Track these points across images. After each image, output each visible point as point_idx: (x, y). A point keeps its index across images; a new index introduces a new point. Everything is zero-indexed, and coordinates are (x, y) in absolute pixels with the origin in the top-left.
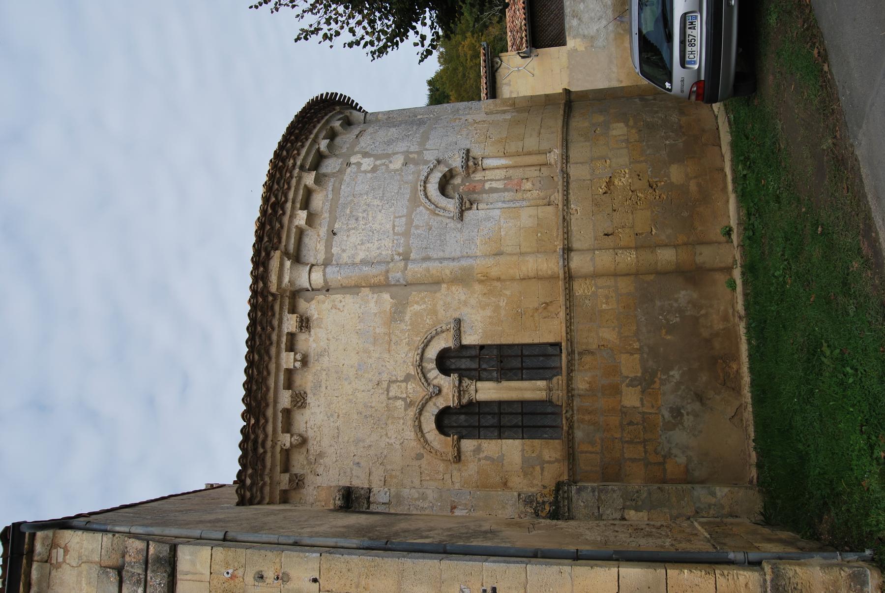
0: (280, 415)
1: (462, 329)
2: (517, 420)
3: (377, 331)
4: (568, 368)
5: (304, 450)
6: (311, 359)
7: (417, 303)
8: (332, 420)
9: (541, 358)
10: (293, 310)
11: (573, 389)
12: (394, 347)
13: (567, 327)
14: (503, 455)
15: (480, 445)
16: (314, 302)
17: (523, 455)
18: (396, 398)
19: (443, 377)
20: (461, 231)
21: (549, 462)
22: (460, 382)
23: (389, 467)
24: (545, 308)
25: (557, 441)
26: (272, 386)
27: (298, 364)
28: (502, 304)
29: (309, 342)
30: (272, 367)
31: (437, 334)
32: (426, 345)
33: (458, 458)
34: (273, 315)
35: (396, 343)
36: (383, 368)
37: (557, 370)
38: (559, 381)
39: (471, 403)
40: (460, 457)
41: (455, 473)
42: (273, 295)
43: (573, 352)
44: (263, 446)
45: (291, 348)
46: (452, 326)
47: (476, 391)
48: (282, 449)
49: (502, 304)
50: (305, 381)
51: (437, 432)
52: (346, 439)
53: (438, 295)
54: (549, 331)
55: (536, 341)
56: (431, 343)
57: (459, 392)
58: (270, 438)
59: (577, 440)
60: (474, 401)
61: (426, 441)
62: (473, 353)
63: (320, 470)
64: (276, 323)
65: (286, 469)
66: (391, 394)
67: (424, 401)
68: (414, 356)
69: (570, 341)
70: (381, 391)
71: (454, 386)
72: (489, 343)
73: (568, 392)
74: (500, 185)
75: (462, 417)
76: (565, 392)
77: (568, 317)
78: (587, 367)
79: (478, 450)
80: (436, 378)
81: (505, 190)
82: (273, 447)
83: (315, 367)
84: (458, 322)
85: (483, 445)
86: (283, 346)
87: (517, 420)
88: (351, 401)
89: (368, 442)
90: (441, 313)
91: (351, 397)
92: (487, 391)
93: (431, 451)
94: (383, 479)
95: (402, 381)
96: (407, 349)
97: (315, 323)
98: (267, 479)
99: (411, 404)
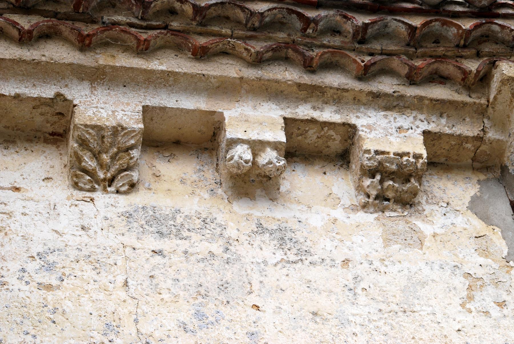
0: (48, 92)
6: (261, 211)
8: (32, 266)
26: (160, 64)
29: (321, 203)
30: (229, 69)
42: (484, 79)
50: (176, 186)
64: (386, 85)
83: (237, 217)
86: (304, 111)
97: (401, 226)
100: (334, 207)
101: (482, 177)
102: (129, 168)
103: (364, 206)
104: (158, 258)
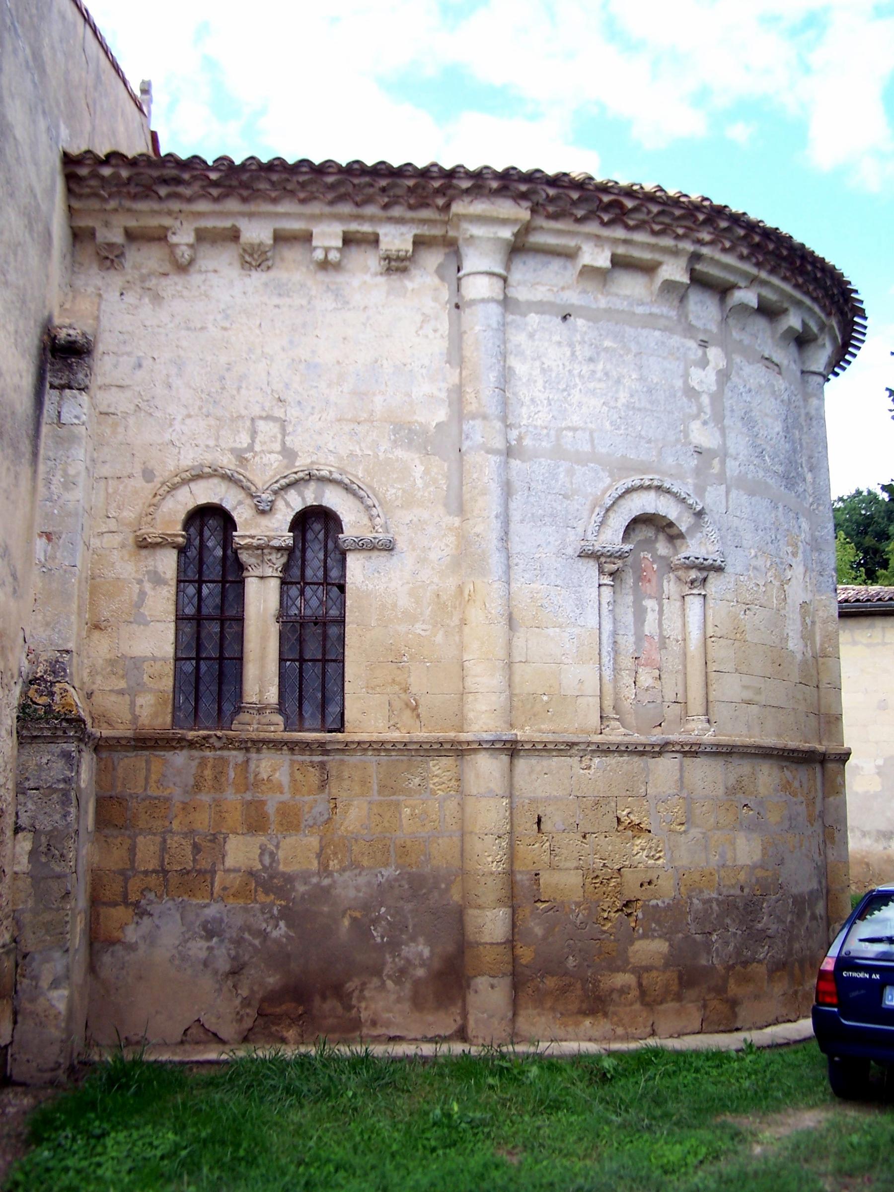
0: (227, 224)
1: (375, 553)
2: (211, 650)
3: (378, 400)
4: (297, 743)
5: (167, 267)
7: (427, 472)
8: (219, 317)
9: (319, 695)
10: (419, 242)
11: (259, 751)
12: (347, 428)
13: (371, 743)
14: (146, 624)
15: (165, 583)
16: (436, 280)
17: (144, 659)
18: (254, 433)
19: (290, 518)
20: (560, 553)
21: (133, 704)
22: (279, 549)
23: (131, 421)
24: (407, 705)
25: (169, 719)
27: (319, 255)
28: (419, 628)
31: (368, 508)
32: (347, 488)
33: (144, 545)
34: (411, 207)
35: (353, 433)
36: (309, 410)
37: (295, 721)
39: (241, 567)
40: (145, 547)
41: (117, 539)
42: (447, 207)
43: (326, 752)
44: (170, 196)
45: (348, 240)
46: (381, 536)
47: (262, 578)
48: (166, 229)
49: (419, 628)
51: (191, 506)
52: (184, 344)
53: (441, 510)
54: (366, 711)
55: (347, 686)
56: (351, 497)
57: (258, 547)
58: (185, 207)
59: (169, 755)
60: (245, 574)
61: (174, 487)
62: (334, 574)
63: (130, 298)
64: (397, 211)
65: (131, 236)
66: (261, 425)
67: (245, 483)
69: (347, 748)
70: (267, 405)
71: (270, 539)
72: (348, 603)
73: (254, 742)
74: (650, 626)
75: (219, 552)
76: (254, 736)
77: (389, 747)
78: (298, 776)
79: (157, 580)
80: (288, 505)
81: (640, 637)
82: (170, 213)
83: (316, 283)
84: (389, 547)
87: (211, 650)
88: (251, 350)
89: (177, 382)
90: (405, 516)
91: (259, 351)
93: (158, 498)
94: (112, 410)
95: (283, 443)
96: (344, 453)
98: (112, 204)
99: (242, 460)
100: (366, 273)
101: (447, 250)
102: (267, 260)
103: (381, 274)
104: (277, 311)
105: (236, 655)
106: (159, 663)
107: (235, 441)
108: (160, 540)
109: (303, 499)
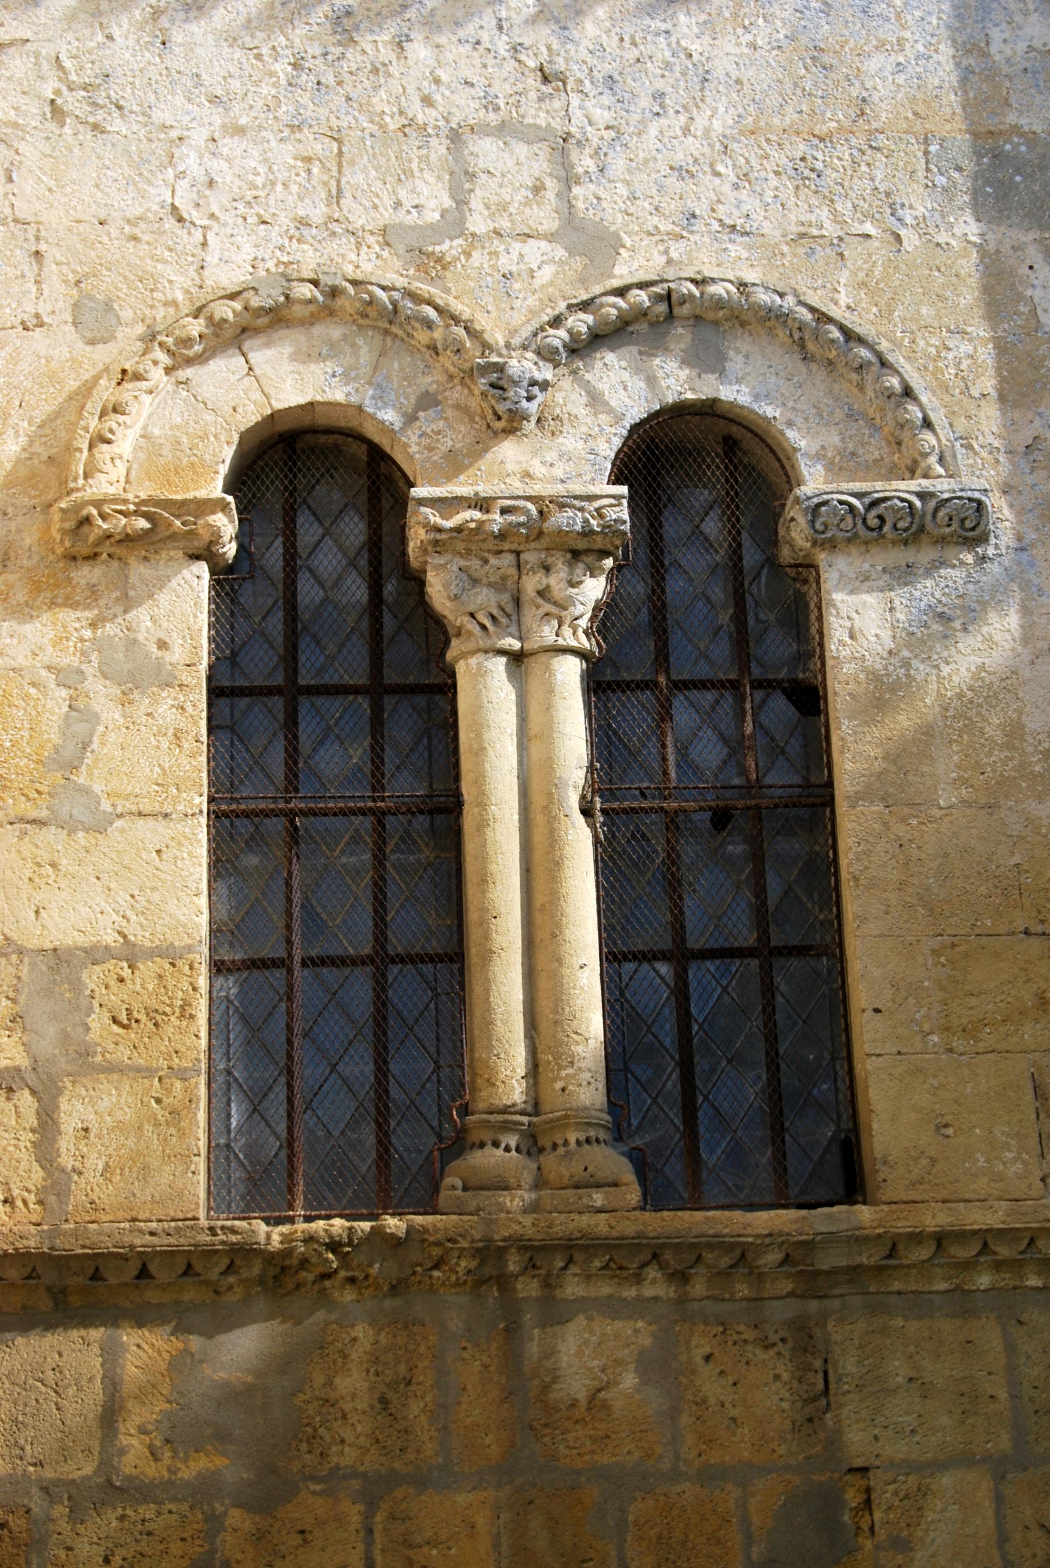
18: (462, 179)
21: (47, 1125)
23: (30, 150)
38: (613, 1203)
46: (943, 486)
51: (251, 416)
66: (486, 151)
68: (726, 267)
70: (501, 90)
79: (137, 678)
80: (596, 400)
85: (168, 698)
92: (527, 733)
105: (434, 946)
106: (148, 969)
107: (398, 204)
108: (143, 524)
109: (651, 381)
